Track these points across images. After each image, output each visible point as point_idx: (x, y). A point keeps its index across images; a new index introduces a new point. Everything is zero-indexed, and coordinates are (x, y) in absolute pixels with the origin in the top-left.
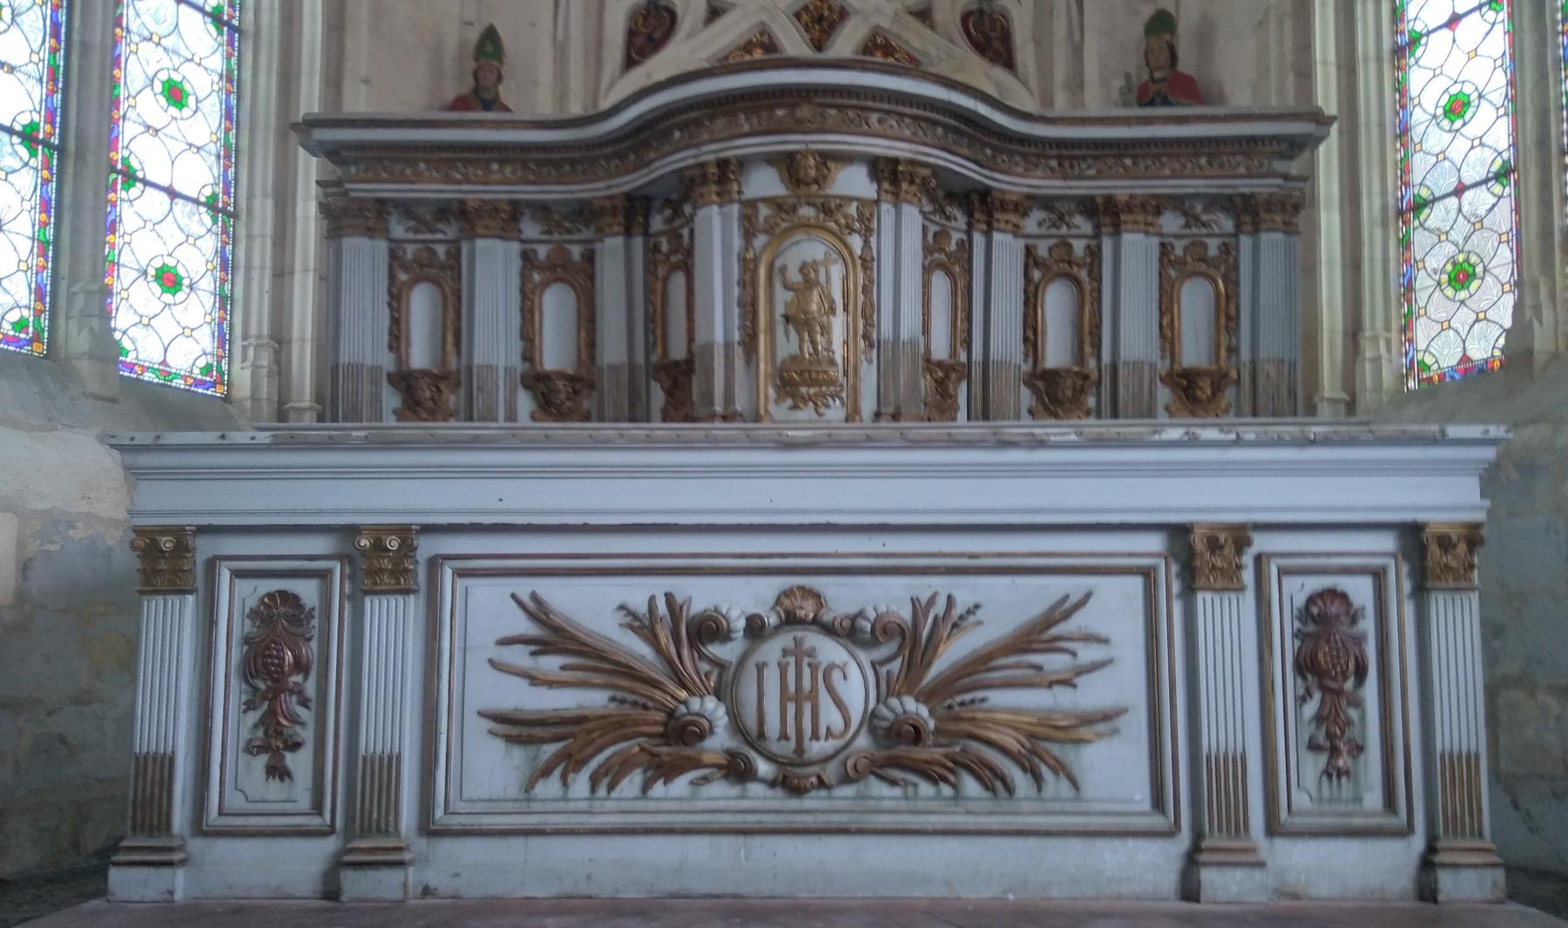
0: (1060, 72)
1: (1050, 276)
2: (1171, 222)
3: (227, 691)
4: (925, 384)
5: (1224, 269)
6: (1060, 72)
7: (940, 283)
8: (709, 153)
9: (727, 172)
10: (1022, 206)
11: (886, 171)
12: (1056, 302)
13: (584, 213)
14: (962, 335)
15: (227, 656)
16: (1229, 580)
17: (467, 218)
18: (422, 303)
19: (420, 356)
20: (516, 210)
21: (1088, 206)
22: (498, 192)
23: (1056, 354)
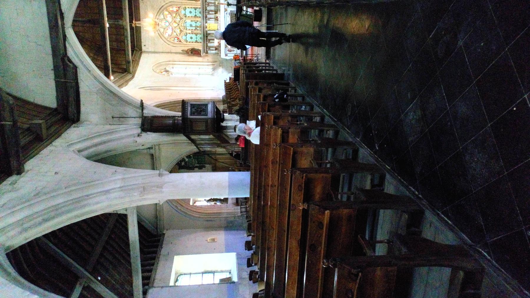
0: (181, 4)
1: (209, 13)
2: (206, 6)
3: (231, 52)
4: (216, 21)
5: (209, 3)
6: (181, 4)
7: (210, 20)
8: (205, 32)
9: (206, 31)
10: (206, 15)
11: (206, 23)
12: (211, 13)
13: (206, 40)
14: (213, 18)
15: (230, 53)
16: (227, 9)
17: (207, 46)
18: (211, 49)
19: (214, 49)
20: (206, 43)
21: (205, 11)
22: (205, 44)
23: (214, 13)
